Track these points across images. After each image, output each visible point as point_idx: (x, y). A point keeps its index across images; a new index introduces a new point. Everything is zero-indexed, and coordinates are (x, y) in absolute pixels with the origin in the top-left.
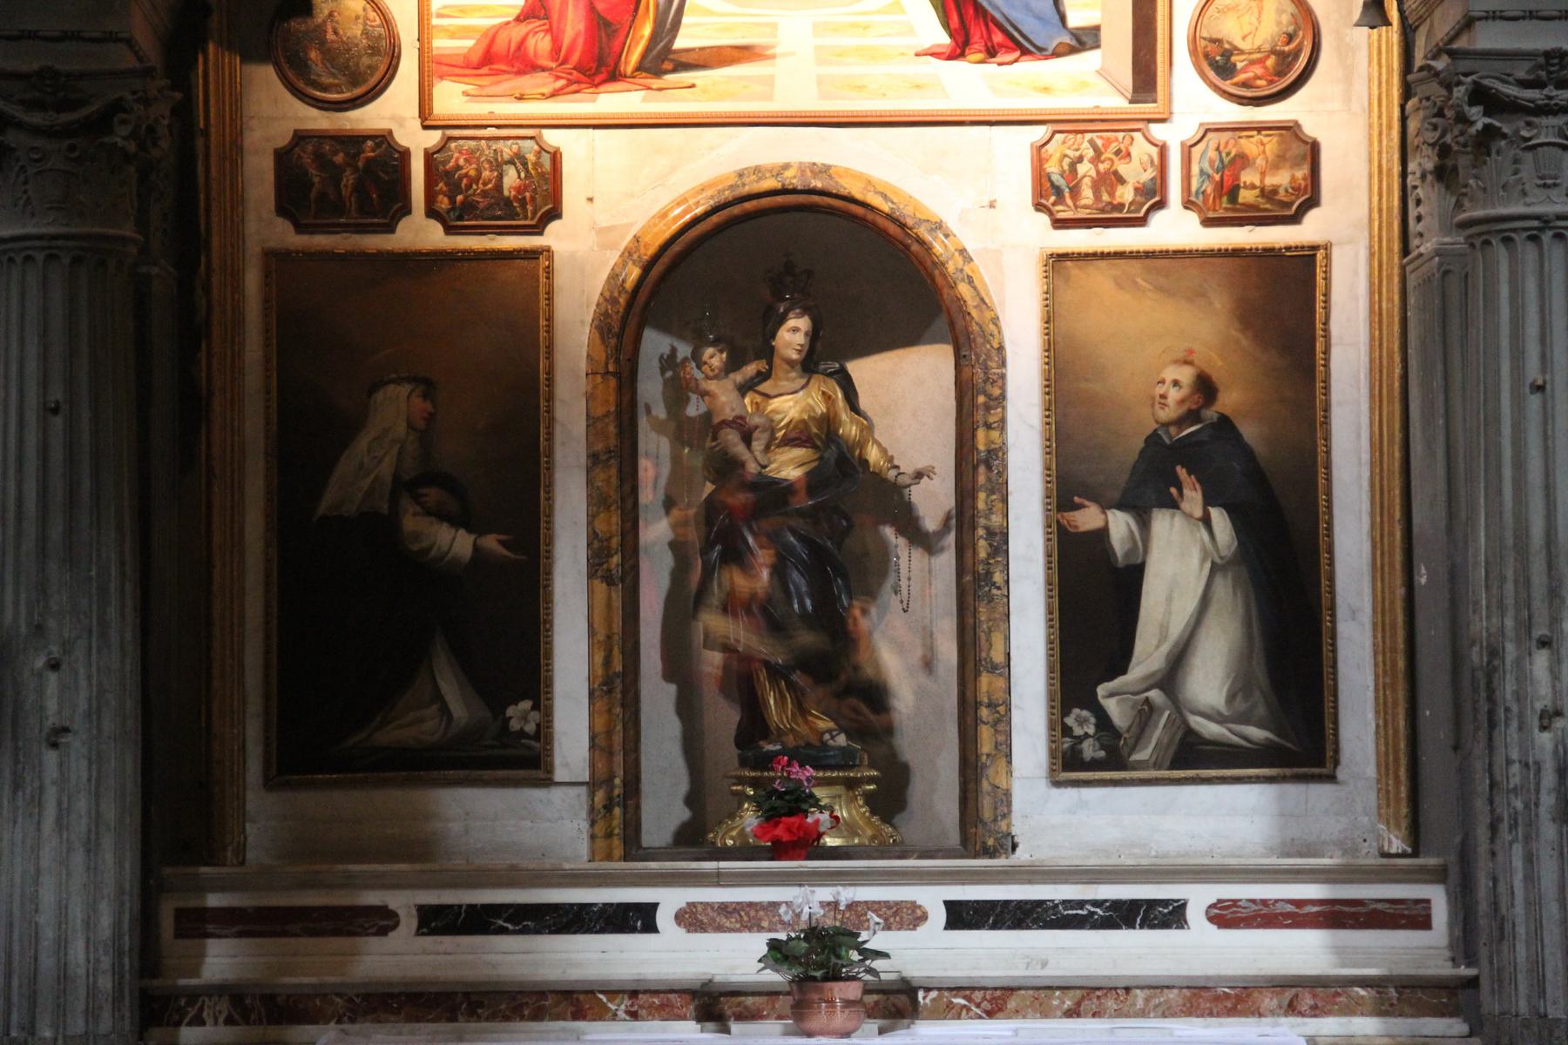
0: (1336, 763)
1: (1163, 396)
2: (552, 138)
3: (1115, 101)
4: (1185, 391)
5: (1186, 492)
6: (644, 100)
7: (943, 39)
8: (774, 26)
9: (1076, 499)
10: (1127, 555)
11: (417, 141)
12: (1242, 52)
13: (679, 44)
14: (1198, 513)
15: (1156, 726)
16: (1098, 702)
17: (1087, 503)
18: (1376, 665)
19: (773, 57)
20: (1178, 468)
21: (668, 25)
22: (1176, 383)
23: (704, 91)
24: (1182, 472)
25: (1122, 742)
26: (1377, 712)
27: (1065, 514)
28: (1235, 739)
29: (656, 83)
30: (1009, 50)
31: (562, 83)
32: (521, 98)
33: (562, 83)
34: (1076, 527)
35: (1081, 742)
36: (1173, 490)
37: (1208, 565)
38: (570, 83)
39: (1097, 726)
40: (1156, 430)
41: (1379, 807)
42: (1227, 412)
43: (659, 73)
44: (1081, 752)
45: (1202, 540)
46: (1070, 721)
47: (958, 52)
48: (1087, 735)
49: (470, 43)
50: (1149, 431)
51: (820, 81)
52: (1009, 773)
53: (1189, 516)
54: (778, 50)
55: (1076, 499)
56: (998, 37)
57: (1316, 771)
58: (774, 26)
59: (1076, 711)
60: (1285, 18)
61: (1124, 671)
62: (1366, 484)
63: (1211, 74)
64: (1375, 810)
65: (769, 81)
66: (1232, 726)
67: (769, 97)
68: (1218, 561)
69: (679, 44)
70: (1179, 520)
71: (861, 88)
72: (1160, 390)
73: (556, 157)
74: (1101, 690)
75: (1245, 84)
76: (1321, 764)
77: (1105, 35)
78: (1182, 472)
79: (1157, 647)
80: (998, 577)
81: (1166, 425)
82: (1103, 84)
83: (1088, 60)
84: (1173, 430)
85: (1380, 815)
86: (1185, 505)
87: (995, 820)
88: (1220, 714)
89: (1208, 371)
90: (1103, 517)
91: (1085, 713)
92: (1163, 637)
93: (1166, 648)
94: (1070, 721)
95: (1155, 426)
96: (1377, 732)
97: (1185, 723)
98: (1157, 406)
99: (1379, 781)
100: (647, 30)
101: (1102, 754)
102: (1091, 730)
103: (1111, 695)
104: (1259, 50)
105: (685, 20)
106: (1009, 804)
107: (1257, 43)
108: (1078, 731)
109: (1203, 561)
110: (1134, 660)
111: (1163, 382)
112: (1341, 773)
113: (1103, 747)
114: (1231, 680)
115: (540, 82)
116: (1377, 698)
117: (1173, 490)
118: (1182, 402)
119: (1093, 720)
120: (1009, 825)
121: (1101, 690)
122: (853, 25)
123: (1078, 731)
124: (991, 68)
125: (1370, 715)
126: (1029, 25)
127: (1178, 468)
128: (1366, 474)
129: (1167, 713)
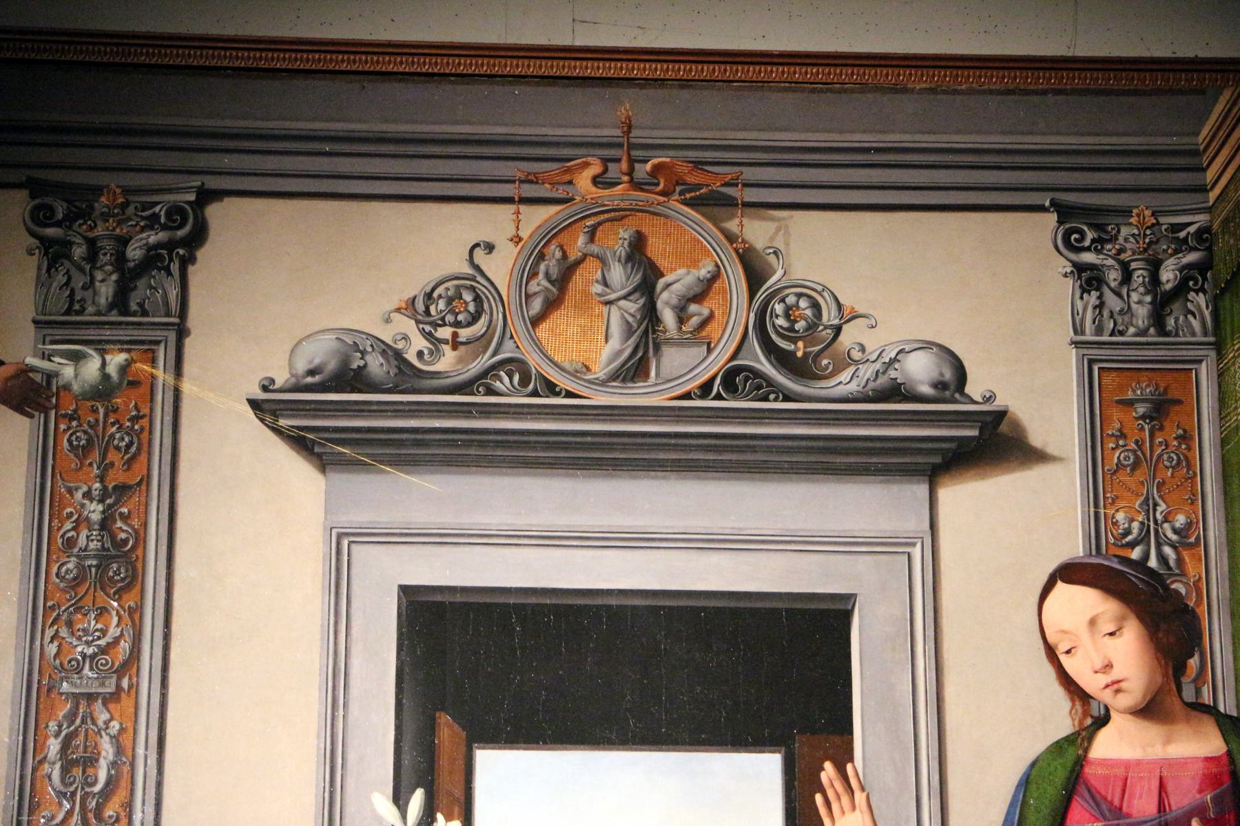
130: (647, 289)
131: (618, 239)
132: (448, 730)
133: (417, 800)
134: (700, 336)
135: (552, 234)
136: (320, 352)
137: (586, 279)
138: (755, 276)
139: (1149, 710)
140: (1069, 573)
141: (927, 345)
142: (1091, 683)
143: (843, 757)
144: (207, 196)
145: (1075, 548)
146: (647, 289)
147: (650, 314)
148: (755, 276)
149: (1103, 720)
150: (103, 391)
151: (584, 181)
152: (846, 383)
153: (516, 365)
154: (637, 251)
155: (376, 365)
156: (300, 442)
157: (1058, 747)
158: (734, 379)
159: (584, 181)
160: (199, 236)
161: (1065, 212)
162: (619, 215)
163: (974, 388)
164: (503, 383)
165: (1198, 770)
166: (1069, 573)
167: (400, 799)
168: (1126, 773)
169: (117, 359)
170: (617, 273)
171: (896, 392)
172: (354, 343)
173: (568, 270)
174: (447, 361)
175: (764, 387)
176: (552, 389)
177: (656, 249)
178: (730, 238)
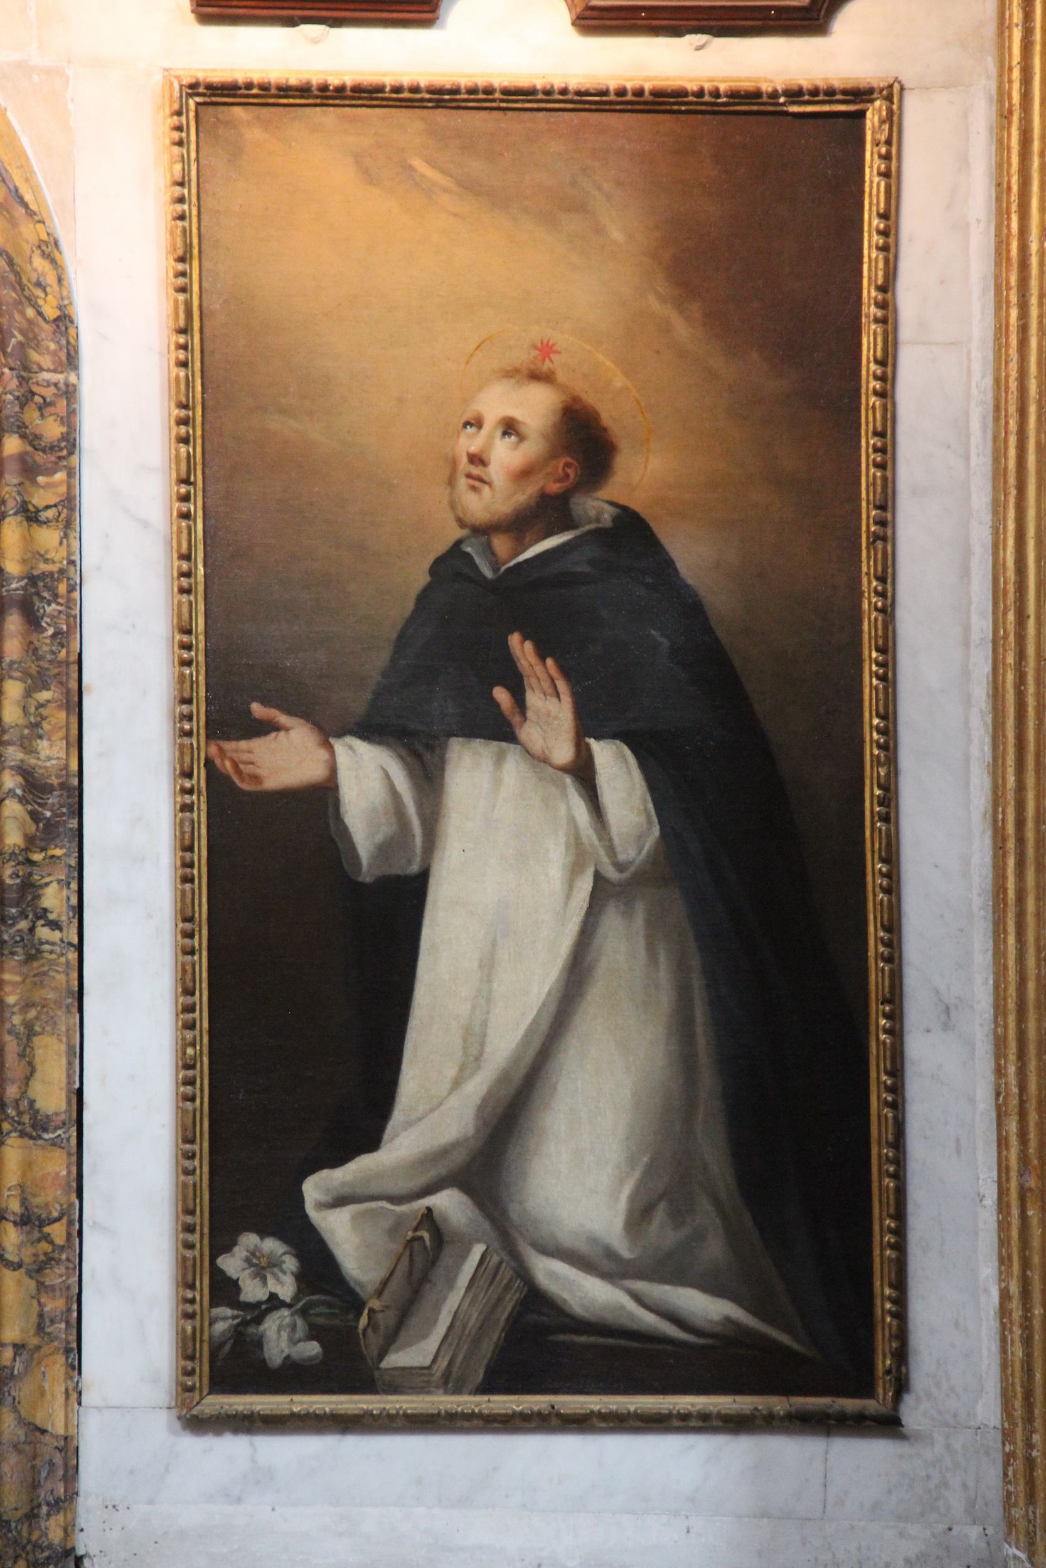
0: (901, 1386)
1: (477, 459)
4: (532, 448)
5: (533, 699)
9: (257, 709)
10: (384, 851)
14: (564, 753)
15: (451, 1283)
16: (305, 1216)
17: (283, 719)
18: (1002, 1142)
20: (514, 639)
22: (510, 427)
24: (522, 649)
25: (364, 1321)
26: (1004, 1261)
27: (228, 746)
28: (649, 1320)
34: (256, 779)
35: (259, 1320)
36: (501, 695)
37: (585, 884)
39: (299, 1277)
40: (458, 543)
41: (1008, 1502)
42: (637, 502)
44: (259, 1343)
45: (572, 820)
46: (232, 1264)
48: (274, 1302)
50: (441, 547)
52: (74, 1395)
53: (540, 760)
55: (257, 709)
57: (850, 1404)
59: (249, 1240)
61: (372, 1143)
62: (981, 692)
64: (997, 1512)
66: (640, 1286)
68: (611, 873)
70: (513, 767)
72: (470, 442)
74: (314, 1188)
76: (866, 1389)
78: (522, 649)
79: (457, 1083)
80: (53, 898)
81: (483, 531)
84: (501, 544)
85: (1011, 1524)
86: (530, 733)
87: (32, 1516)
88: (610, 1254)
89: (591, 399)
90: (323, 754)
91: (272, 1245)
92: (471, 1062)
93: (477, 1087)
94: (232, 1264)
95: (456, 533)
96: (1004, 1312)
97: (524, 1275)
98: (462, 483)
99: (1007, 1436)
101: (313, 1349)
102: (286, 1289)
103: (340, 1201)
106: (71, 1473)
108: (252, 1291)
109: (574, 870)
110: (398, 1115)
111: (477, 423)
112: (912, 1414)
113: (315, 1333)
114: (637, 1175)
116: (1003, 1226)
117: (501, 695)
118: (524, 474)
119: (291, 1264)
120: (69, 1529)
121: (314, 1188)
123: (252, 1291)
125: (988, 1270)
127: (514, 639)
128: (982, 667)
129: (478, 1250)
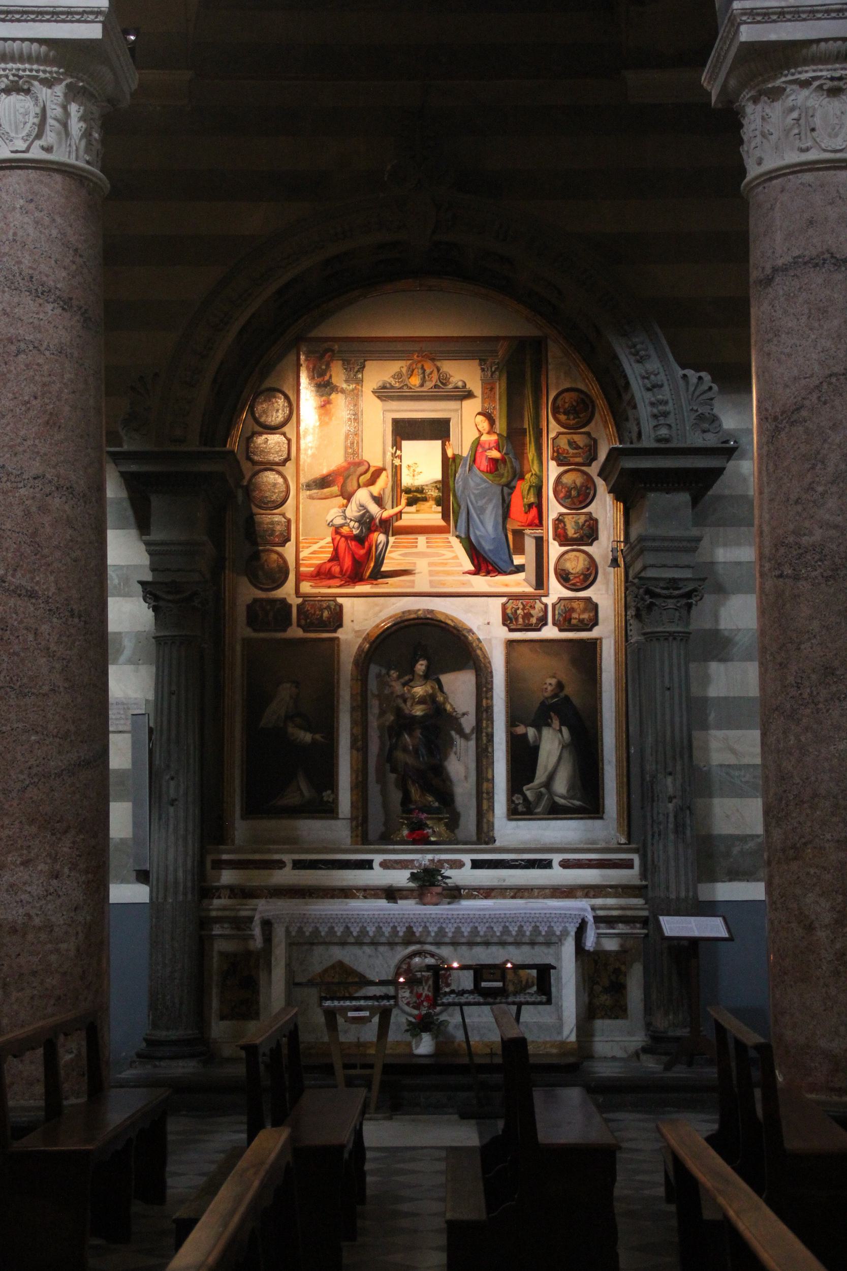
2: (340, 600)
3: (529, 590)
6: (371, 588)
7: (472, 568)
8: (415, 563)
11: (295, 601)
12: (572, 574)
13: (383, 569)
19: (414, 574)
21: (380, 562)
23: (391, 585)
29: (375, 582)
30: (494, 572)
31: (343, 582)
32: (329, 587)
33: (343, 582)
38: (346, 582)
43: (376, 579)
47: (476, 572)
49: (312, 569)
51: (431, 582)
54: (416, 571)
56: (490, 568)
58: (415, 563)
60: (586, 563)
63: (562, 581)
65: (413, 582)
67: (413, 587)
69: (383, 569)
71: (444, 584)
73: (341, 606)
75: (574, 584)
77: (526, 567)
82: (526, 584)
83: (522, 576)
100: (372, 565)
104: (578, 573)
105: (385, 561)
107: (577, 570)
115: (337, 582)
122: (442, 563)
124: (488, 578)
126: (501, 564)
130: (424, 373)
131: (419, 366)
132: (398, 438)
133: (395, 448)
134: (431, 380)
135: (411, 365)
136: (380, 384)
137: (416, 371)
138: (438, 370)
139: (488, 433)
140: (479, 414)
141: (461, 380)
142: (481, 429)
143: (449, 441)
144: (365, 361)
145: (480, 410)
146: (424, 373)
147: (424, 377)
148: (438, 370)
149: (482, 435)
150: (353, 390)
151: (415, 357)
152: (450, 386)
153: (406, 385)
154: (423, 368)
155: (388, 385)
156: (378, 397)
157: (477, 439)
158: (436, 386)
159: (415, 357)
160: (364, 367)
161: (480, 360)
162: (419, 362)
163: (467, 387)
164: (405, 388)
165: (493, 442)
166: (479, 414)
167: (392, 448)
168: (485, 442)
169: (354, 386)
170: (420, 371)
171: (457, 388)
172: (385, 382)
173: (413, 370)
174: (397, 385)
175: (439, 387)
176: (411, 388)
177: (426, 367)
178: (435, 365)
